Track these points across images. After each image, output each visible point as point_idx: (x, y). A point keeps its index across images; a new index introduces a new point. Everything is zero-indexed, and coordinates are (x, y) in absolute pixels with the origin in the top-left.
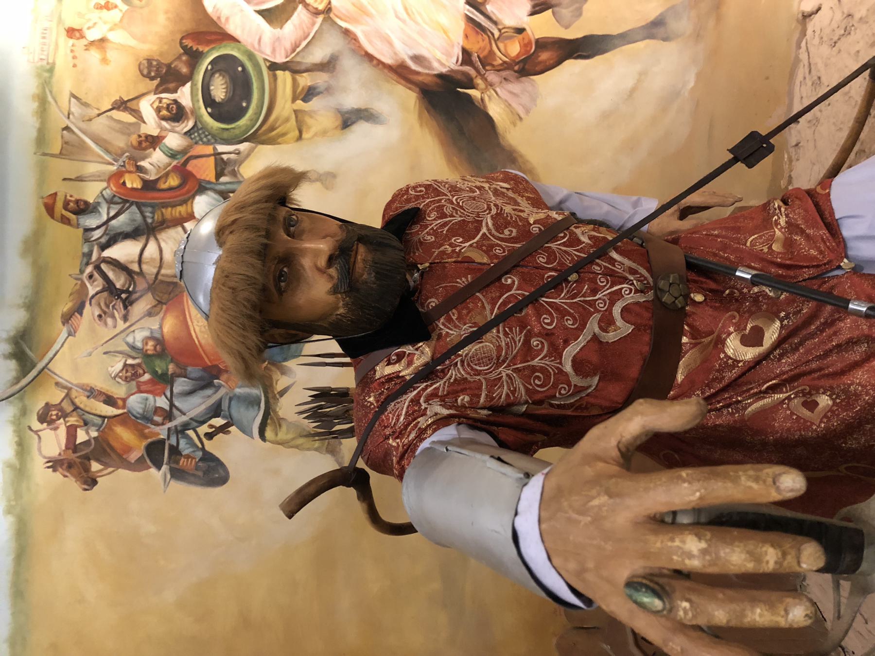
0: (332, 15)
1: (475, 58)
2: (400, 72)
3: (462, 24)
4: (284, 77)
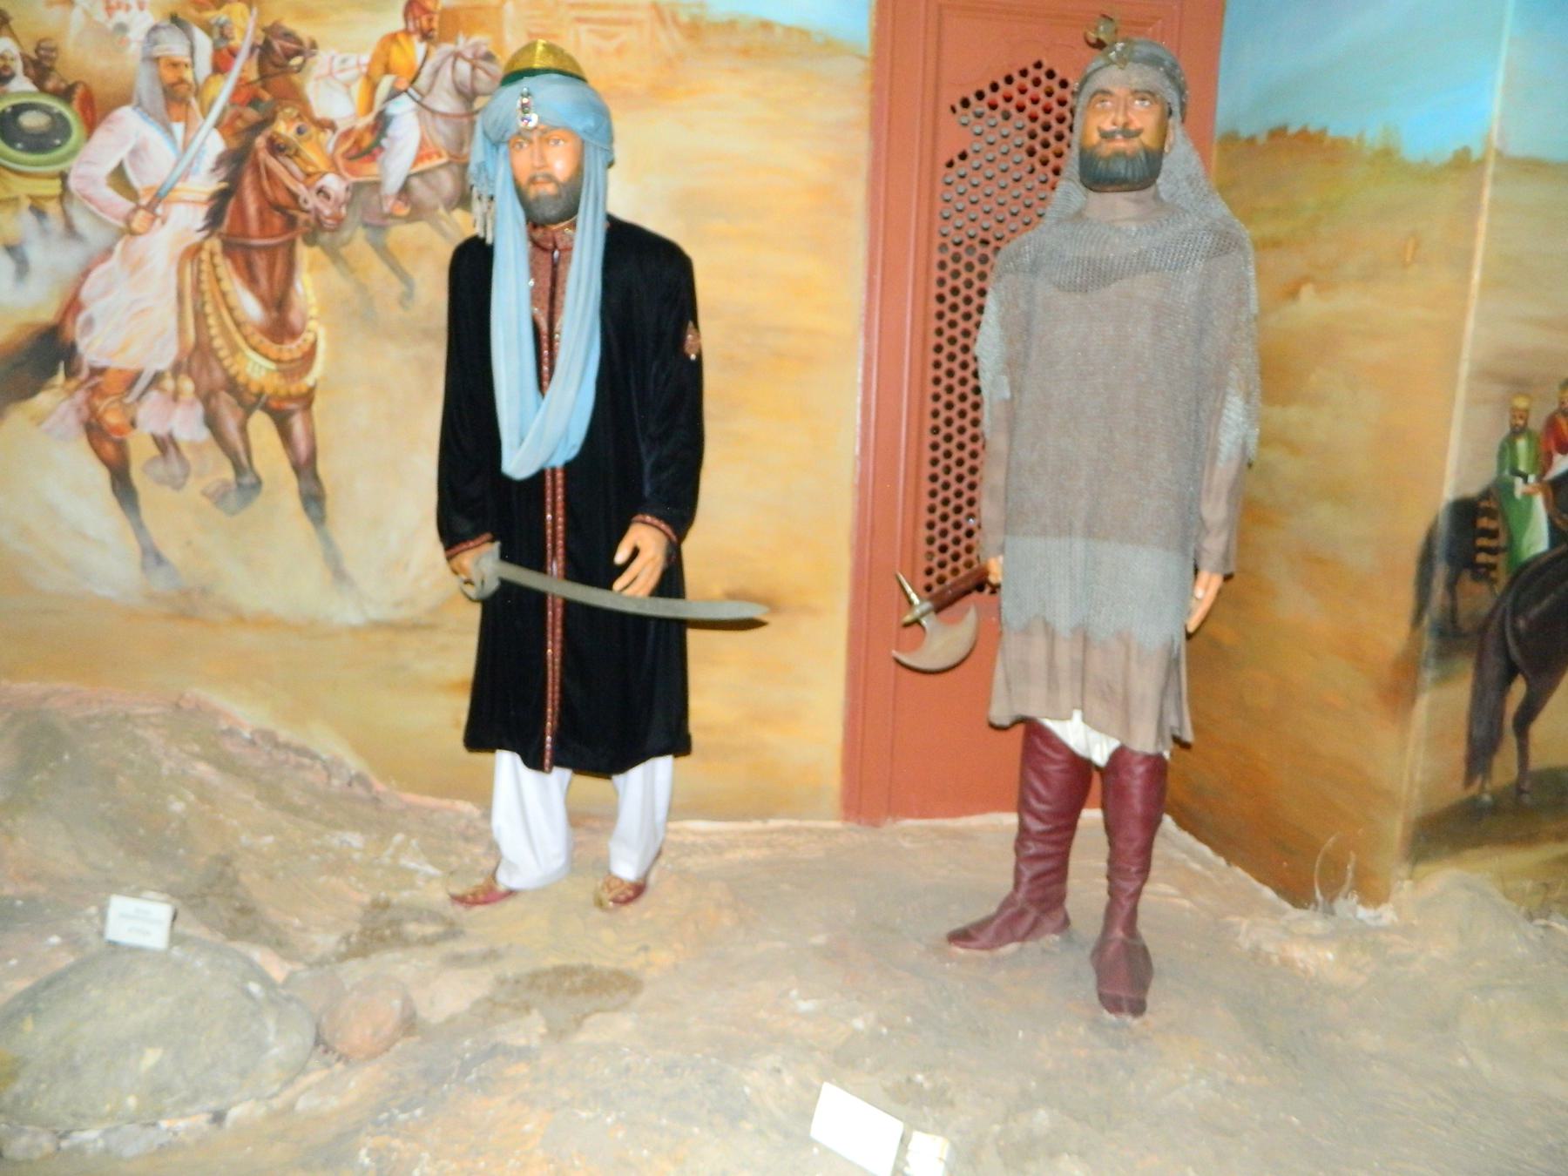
0: (127, 237)
1: (98, 379)
2: (73, 306)
3: (132, 366)
4: (54, 187)
